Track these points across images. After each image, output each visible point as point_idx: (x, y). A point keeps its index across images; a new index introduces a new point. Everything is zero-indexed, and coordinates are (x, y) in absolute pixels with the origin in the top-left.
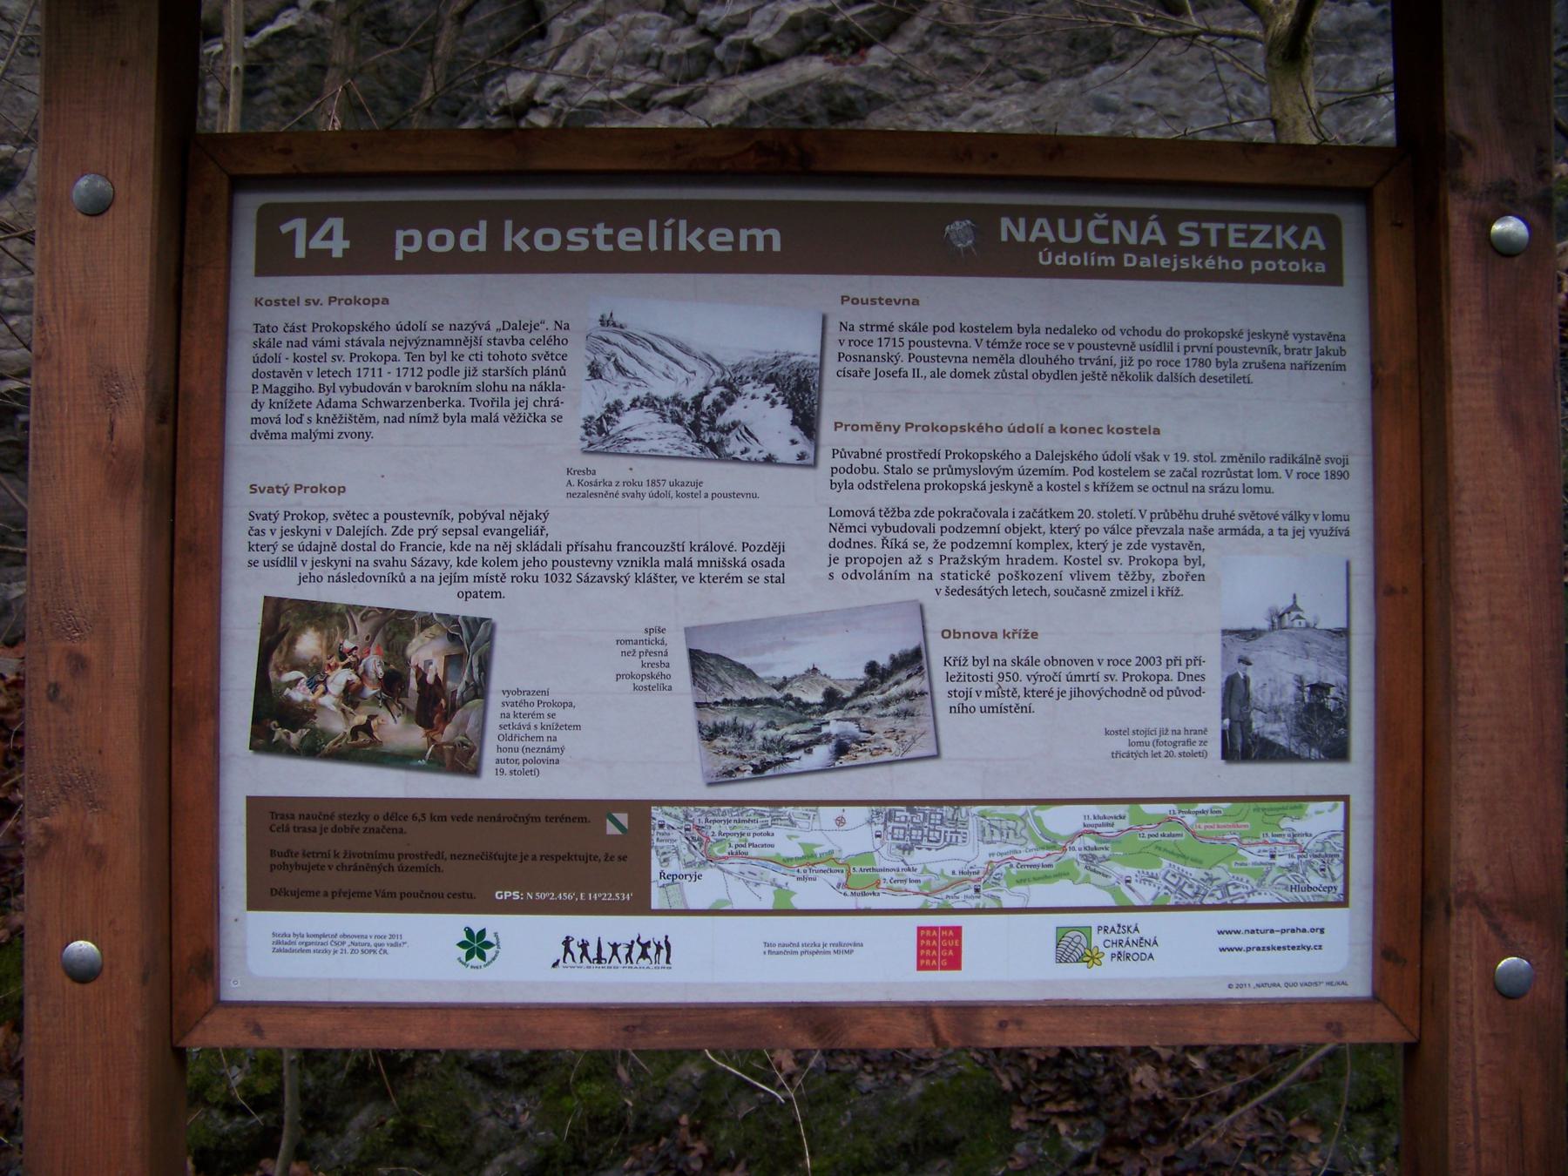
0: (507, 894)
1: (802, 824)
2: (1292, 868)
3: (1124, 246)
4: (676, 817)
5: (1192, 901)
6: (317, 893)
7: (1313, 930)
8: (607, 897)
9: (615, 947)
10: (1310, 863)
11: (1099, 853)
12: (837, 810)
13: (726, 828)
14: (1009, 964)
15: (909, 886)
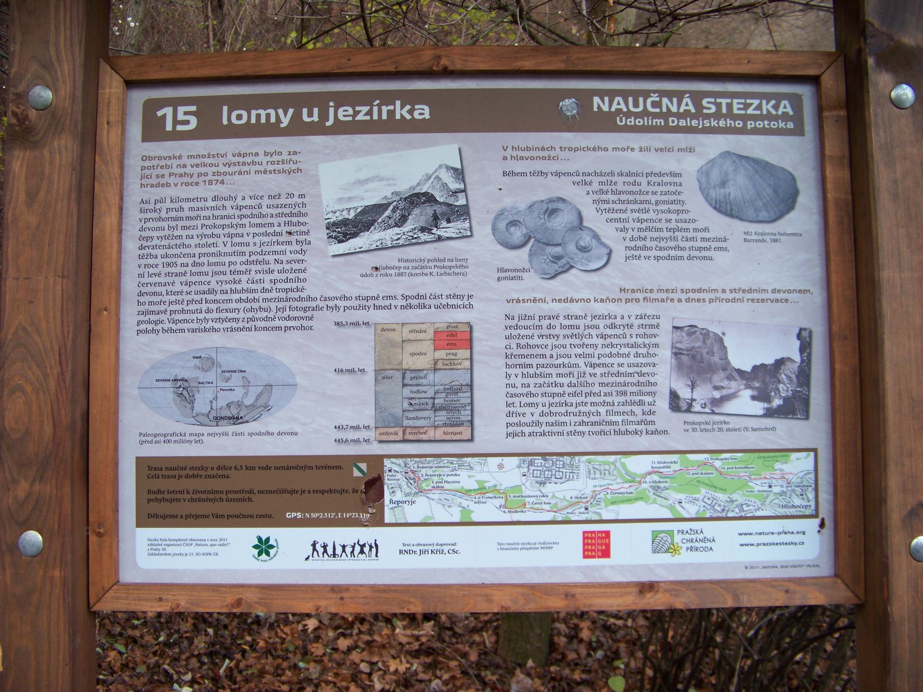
0: (294, 514)
1: (477, 468)
2: (782, 494)
3: (669, 113)
4: (399, 465)
5: (720, 515)
6: (176, 517)
7: (798, 533)
8: (355, 515)
10: (794, 491)
11: (662, 485)
12: (498, 460)
13: (430, 472)
15: (544, 506)
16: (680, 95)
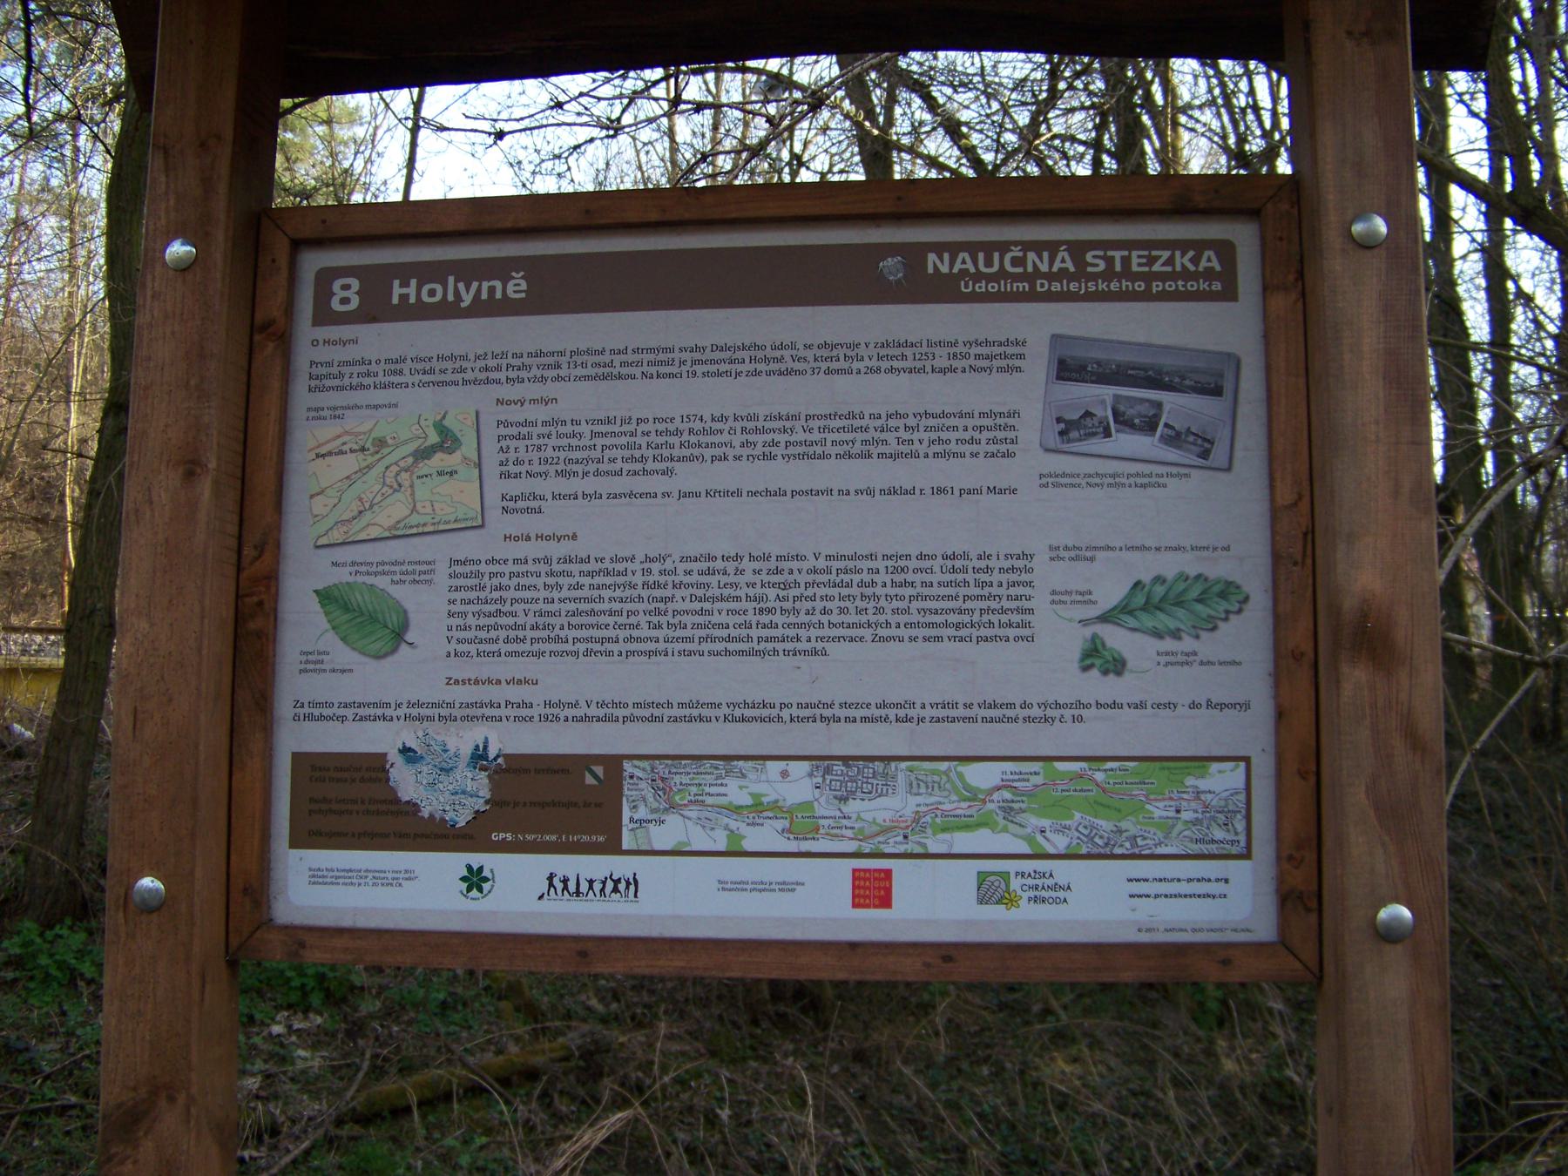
0: (502, 835)
1: (752, 776)
7: (1217, 880)
9: (591, 882)
12: (782, 764)
14: (936, 904)
16: (1052, 247)
